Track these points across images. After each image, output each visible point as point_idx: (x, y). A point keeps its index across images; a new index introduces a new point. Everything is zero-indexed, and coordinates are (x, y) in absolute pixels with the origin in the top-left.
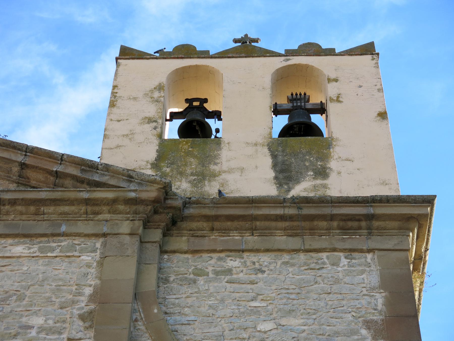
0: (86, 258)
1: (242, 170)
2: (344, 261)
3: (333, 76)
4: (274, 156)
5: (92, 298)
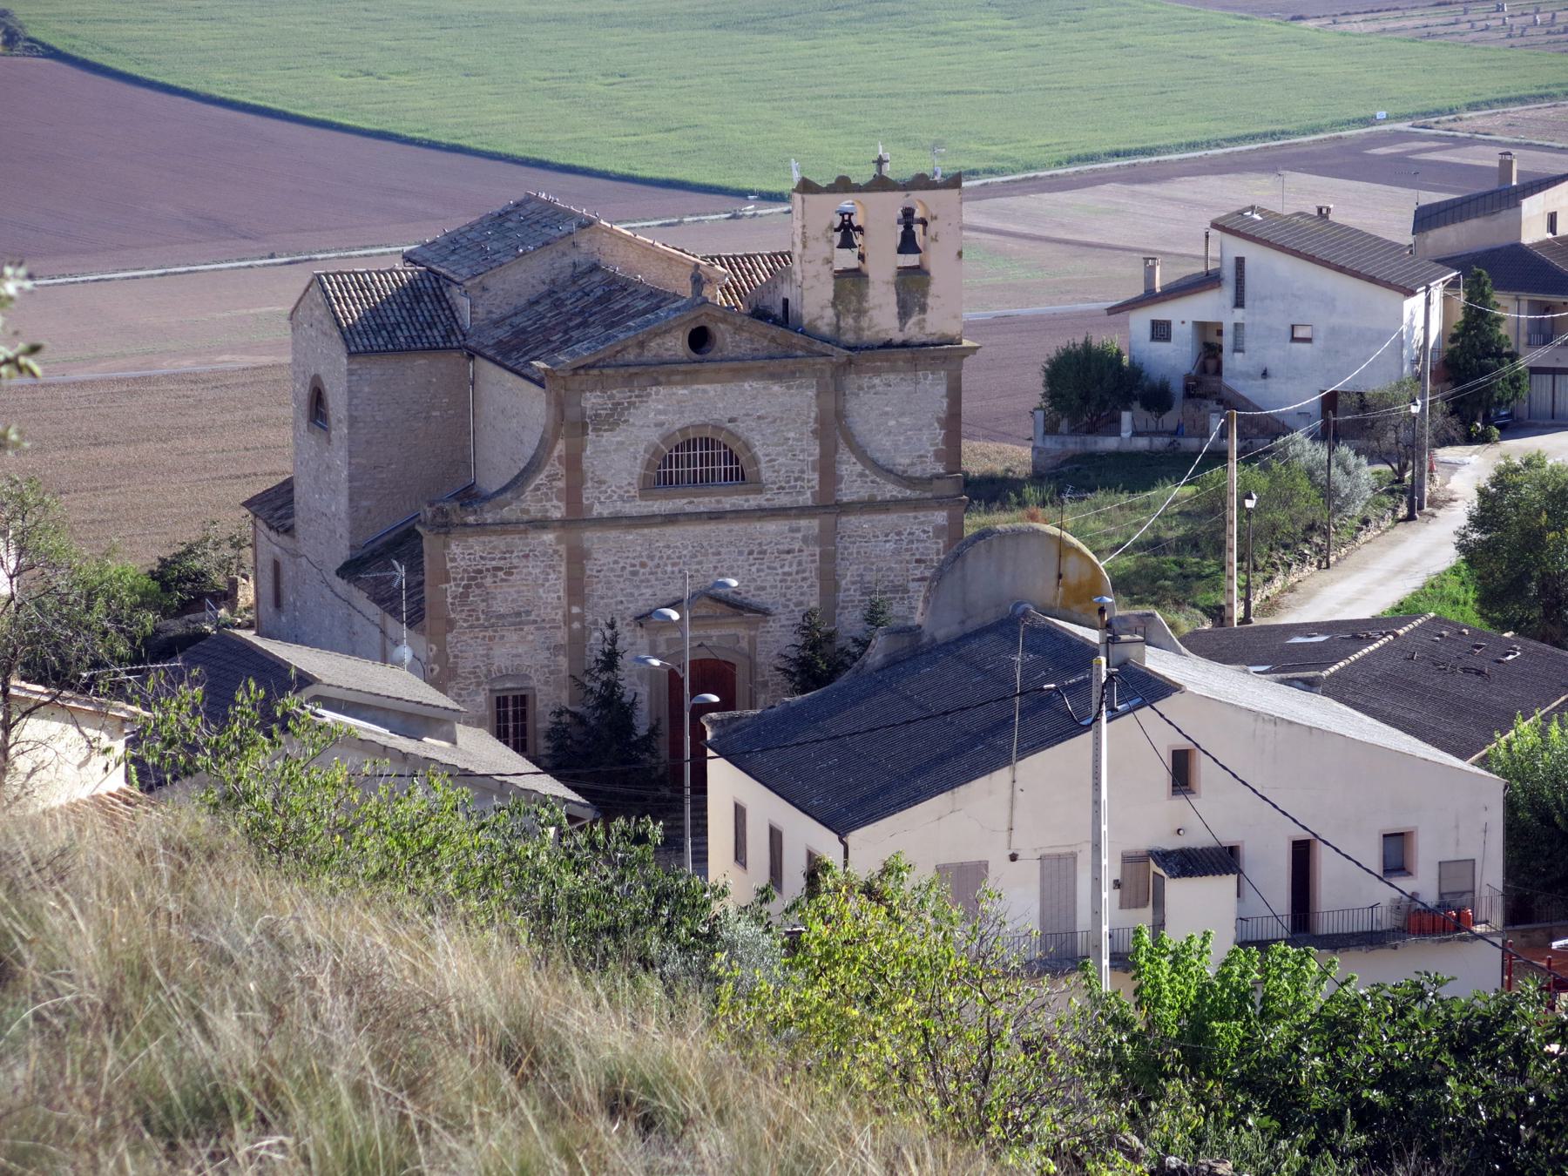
0: (810, 393)
1: (880, 306)
2: (930, 377)
3: (934, 214)
4: (898, 294)
5: (816, 420)
